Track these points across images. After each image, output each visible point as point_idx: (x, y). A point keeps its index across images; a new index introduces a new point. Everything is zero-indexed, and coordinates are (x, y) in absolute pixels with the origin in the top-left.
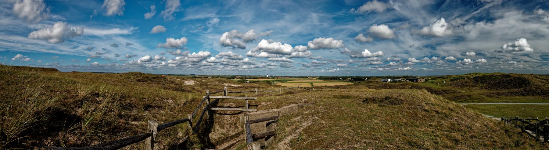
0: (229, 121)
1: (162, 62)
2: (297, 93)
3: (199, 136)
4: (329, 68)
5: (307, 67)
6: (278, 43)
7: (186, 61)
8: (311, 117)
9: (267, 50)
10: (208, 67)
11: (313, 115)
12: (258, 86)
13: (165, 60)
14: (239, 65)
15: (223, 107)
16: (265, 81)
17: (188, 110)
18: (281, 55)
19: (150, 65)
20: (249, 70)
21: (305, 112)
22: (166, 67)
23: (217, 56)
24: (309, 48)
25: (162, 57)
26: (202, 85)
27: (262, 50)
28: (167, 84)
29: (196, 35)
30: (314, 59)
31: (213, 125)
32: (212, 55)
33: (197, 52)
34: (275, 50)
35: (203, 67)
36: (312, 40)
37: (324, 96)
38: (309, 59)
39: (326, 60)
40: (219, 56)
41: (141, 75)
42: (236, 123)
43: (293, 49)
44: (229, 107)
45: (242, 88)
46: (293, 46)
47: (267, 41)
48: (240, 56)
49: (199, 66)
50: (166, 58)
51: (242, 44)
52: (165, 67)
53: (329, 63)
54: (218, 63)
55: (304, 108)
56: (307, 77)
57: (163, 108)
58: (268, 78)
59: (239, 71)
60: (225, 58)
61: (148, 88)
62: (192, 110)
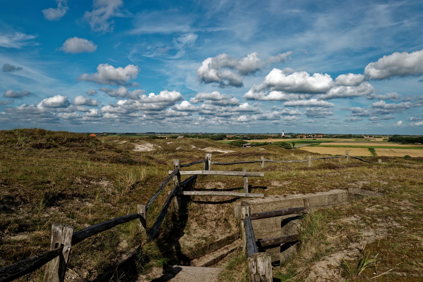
0: (215, 214)
1: (91, 110)
2: (343, 167)
3: (159, 245)
4: (417, 118)
5: (361, 116)
6: (302, 74)
7: (137, 109)
8: (383, 222)
9: (281, 88)
10: (177, 118)
11: (386, 218)
12: (266, 151)
13: (95, 106)
14: (232, 115)
15: (205, 190)
16: (279, 142)
17: (139, 198)
18: (307, 95)
19: (65, 114)
20: (250, 125)
21: (367, 209)
22: (99, 119)
23: (193, 99)
24: (368, 79)
25: (91, 100)
26: (167, 150)
27: (272, 88)
28: (101, 151)
29: (155, 62)
30: (379, 99)
31: (186, 222)
32: (184, 98)
33: (157, 93)
34: (296, 87)
35: (167, 119)
36: (375, 59)
37: (411, 179)
38: (368, 99)
39: (408, 101)
40: (196, 99)
41: (44, 134)
42: (227, 218)
43: (333, 82)
44: (215, 190)
45: (237, 157)
46: (334, 76)
47: (281, 71)
48: (234, 100)
49: (161, 117)
50: (97, 101)
51: (237, 78)
52: (96, 119)
53: (415, 107)
54: (196, 112)
55: (365, 200)
56: (361, 137)
57: (91, 198)
58: (284, 137)
59: (231, 126)
60: (206, 103)
61: (59, 161)
62: (147, 198)
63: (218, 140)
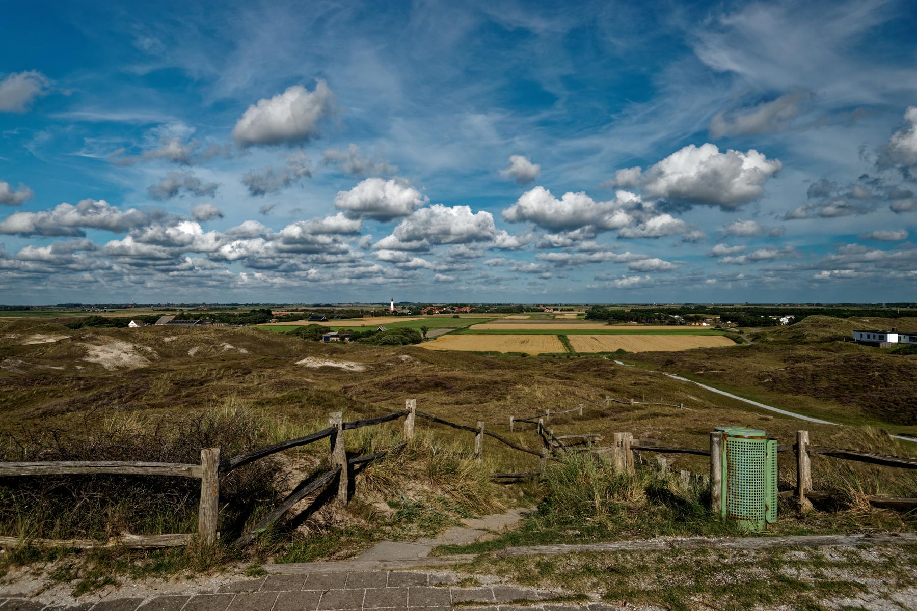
56: (535, 310)
58: (396, 314)
63: (256, 322)
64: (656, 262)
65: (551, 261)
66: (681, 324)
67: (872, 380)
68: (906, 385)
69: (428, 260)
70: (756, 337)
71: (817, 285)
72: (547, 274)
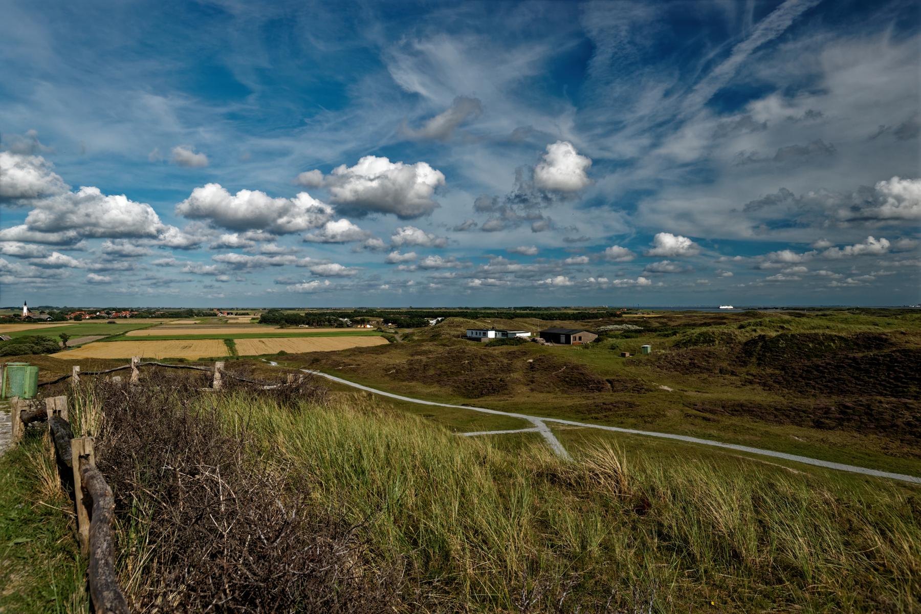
56: (207, 315)
64: (335, 267)
65: (229, 263)
66: (348, 326)
67: (463, 367)
68: (482, 369)
69: (75, 258)
70: (406, 337)
71: (469, 291)
72: (224, 278)
